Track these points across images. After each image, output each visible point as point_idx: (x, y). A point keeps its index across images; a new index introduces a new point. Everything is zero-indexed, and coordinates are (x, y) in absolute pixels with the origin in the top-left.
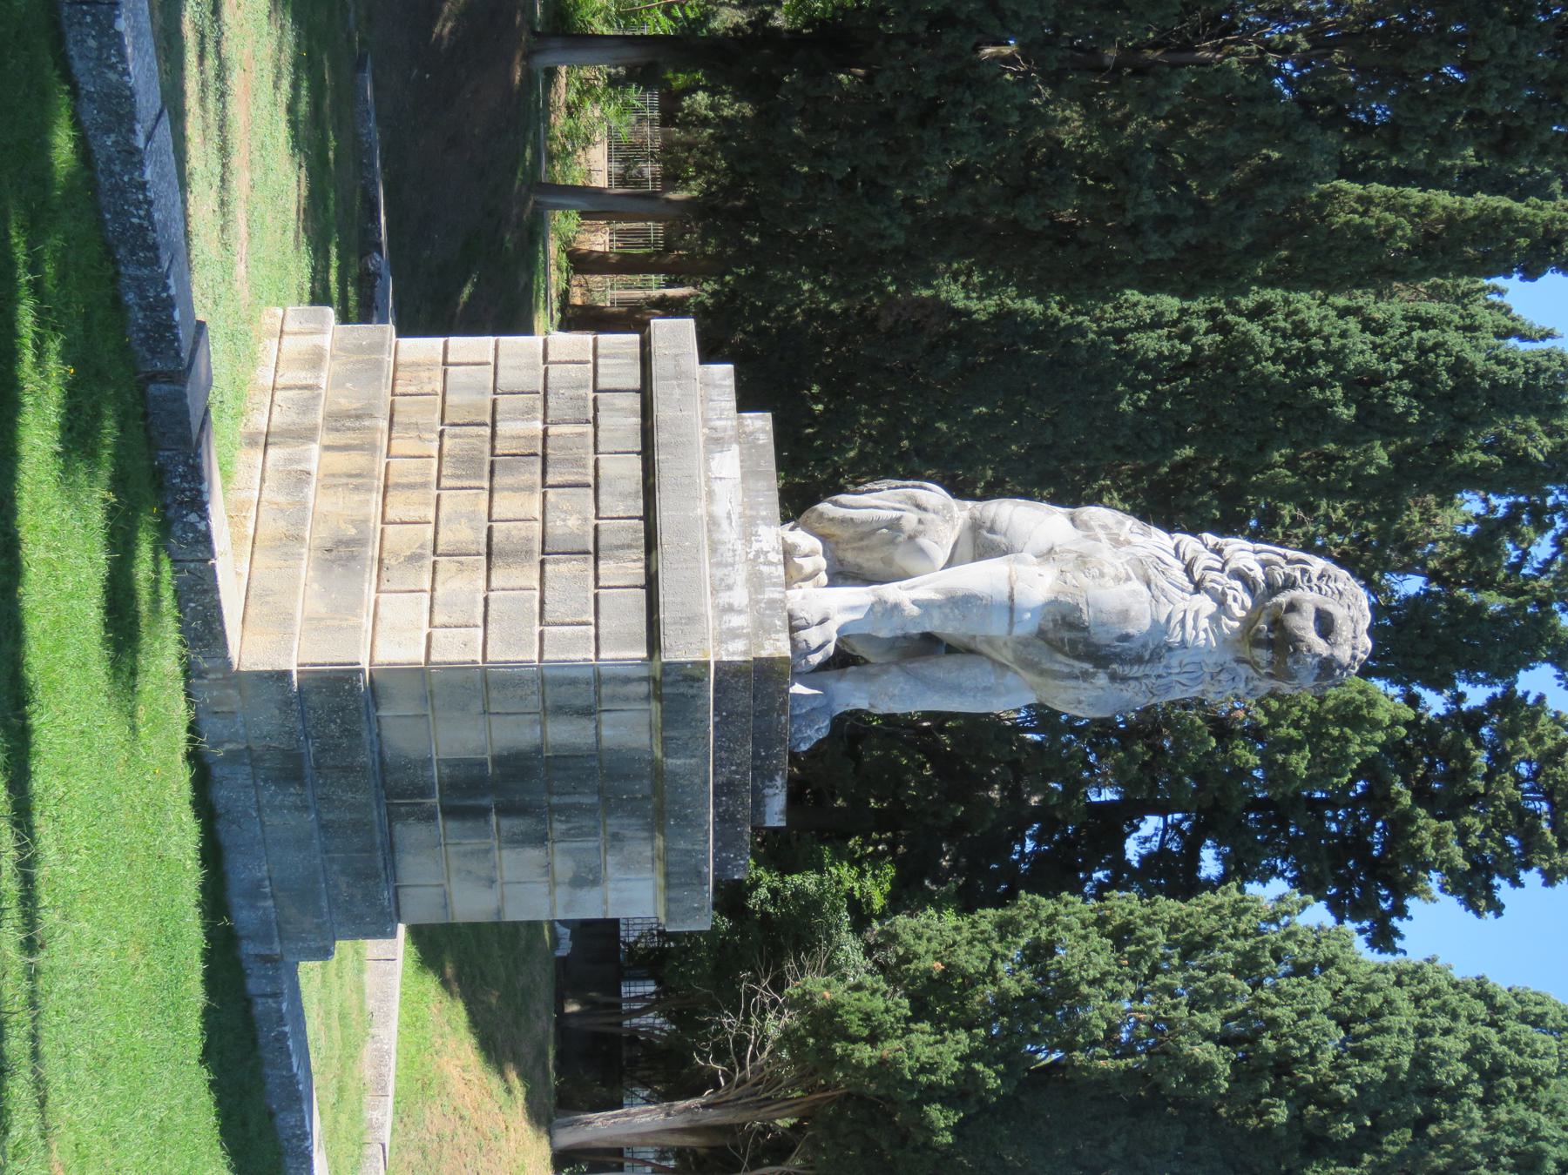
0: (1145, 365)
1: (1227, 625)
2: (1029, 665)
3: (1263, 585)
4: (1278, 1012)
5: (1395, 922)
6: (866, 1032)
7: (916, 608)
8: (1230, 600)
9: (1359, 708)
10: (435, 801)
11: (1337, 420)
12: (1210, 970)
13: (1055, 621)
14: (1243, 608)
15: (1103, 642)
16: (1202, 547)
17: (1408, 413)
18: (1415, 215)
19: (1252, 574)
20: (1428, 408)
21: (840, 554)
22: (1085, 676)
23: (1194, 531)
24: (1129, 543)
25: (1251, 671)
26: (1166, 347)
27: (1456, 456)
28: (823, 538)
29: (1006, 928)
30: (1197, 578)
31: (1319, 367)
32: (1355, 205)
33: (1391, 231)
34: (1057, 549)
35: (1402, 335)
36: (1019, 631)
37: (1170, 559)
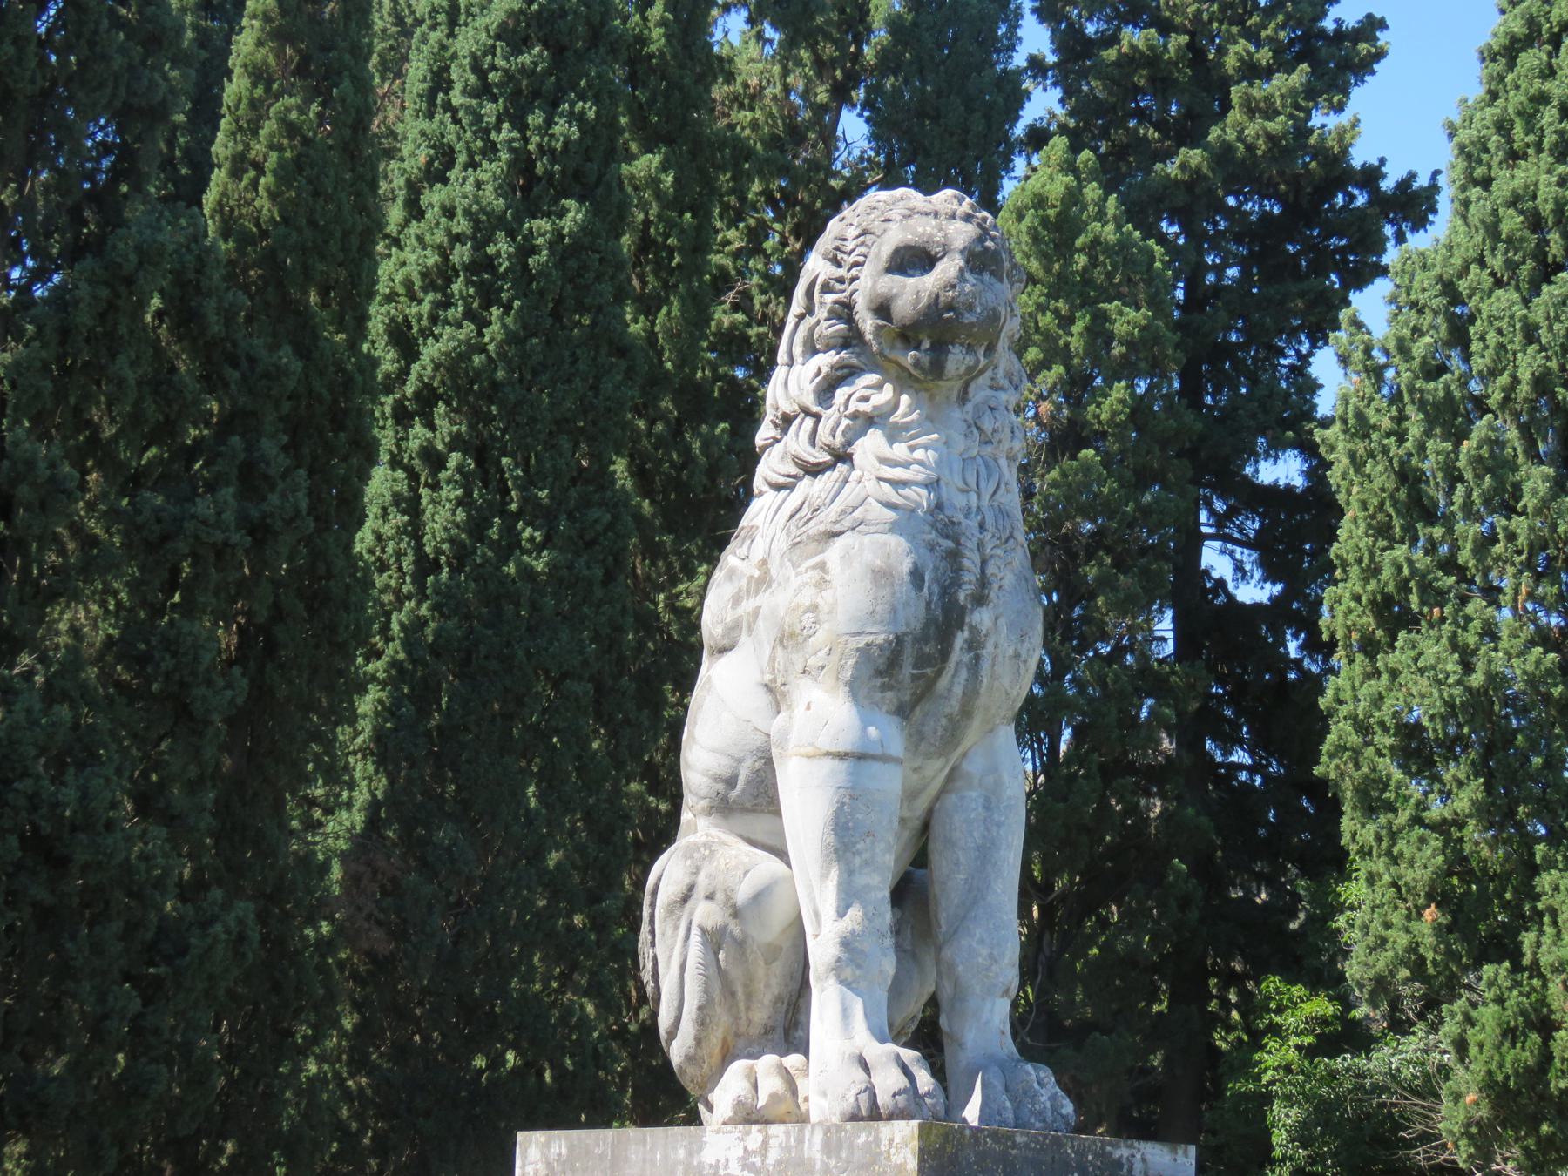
0: (477, 527)
1: (905, 415)
2: (953, 734)
3: (844, 354)
4: (1525, 374)
5: (1387, 185)
6: (1535, 1037)
7: (851, 912)
8: (864, 407)
9: (1045, 221)
11: (585, 229)
12: (1453, 478)
13: (884, 688)
14: (879, 387)
15: (922, 613)
16: (778, 447)
17: (580, 118)
18: (268, 89)
19: (825, 370)
20: (574, 86)
21: (755, 1031)
22: (974, 645)
23: (750, 459)
24: (764, 562)
25: (981, 380)
26: (451, 493)
27: (653, 48)
28: (727, 1058)
29: (1373, 801)
30: (827, 458)
31: (499, 252)
32: (245, 181)
33: (291, 129)
34: (768, 677)
35: (456, 121)
36: (897, 746)
37: (795, 498)
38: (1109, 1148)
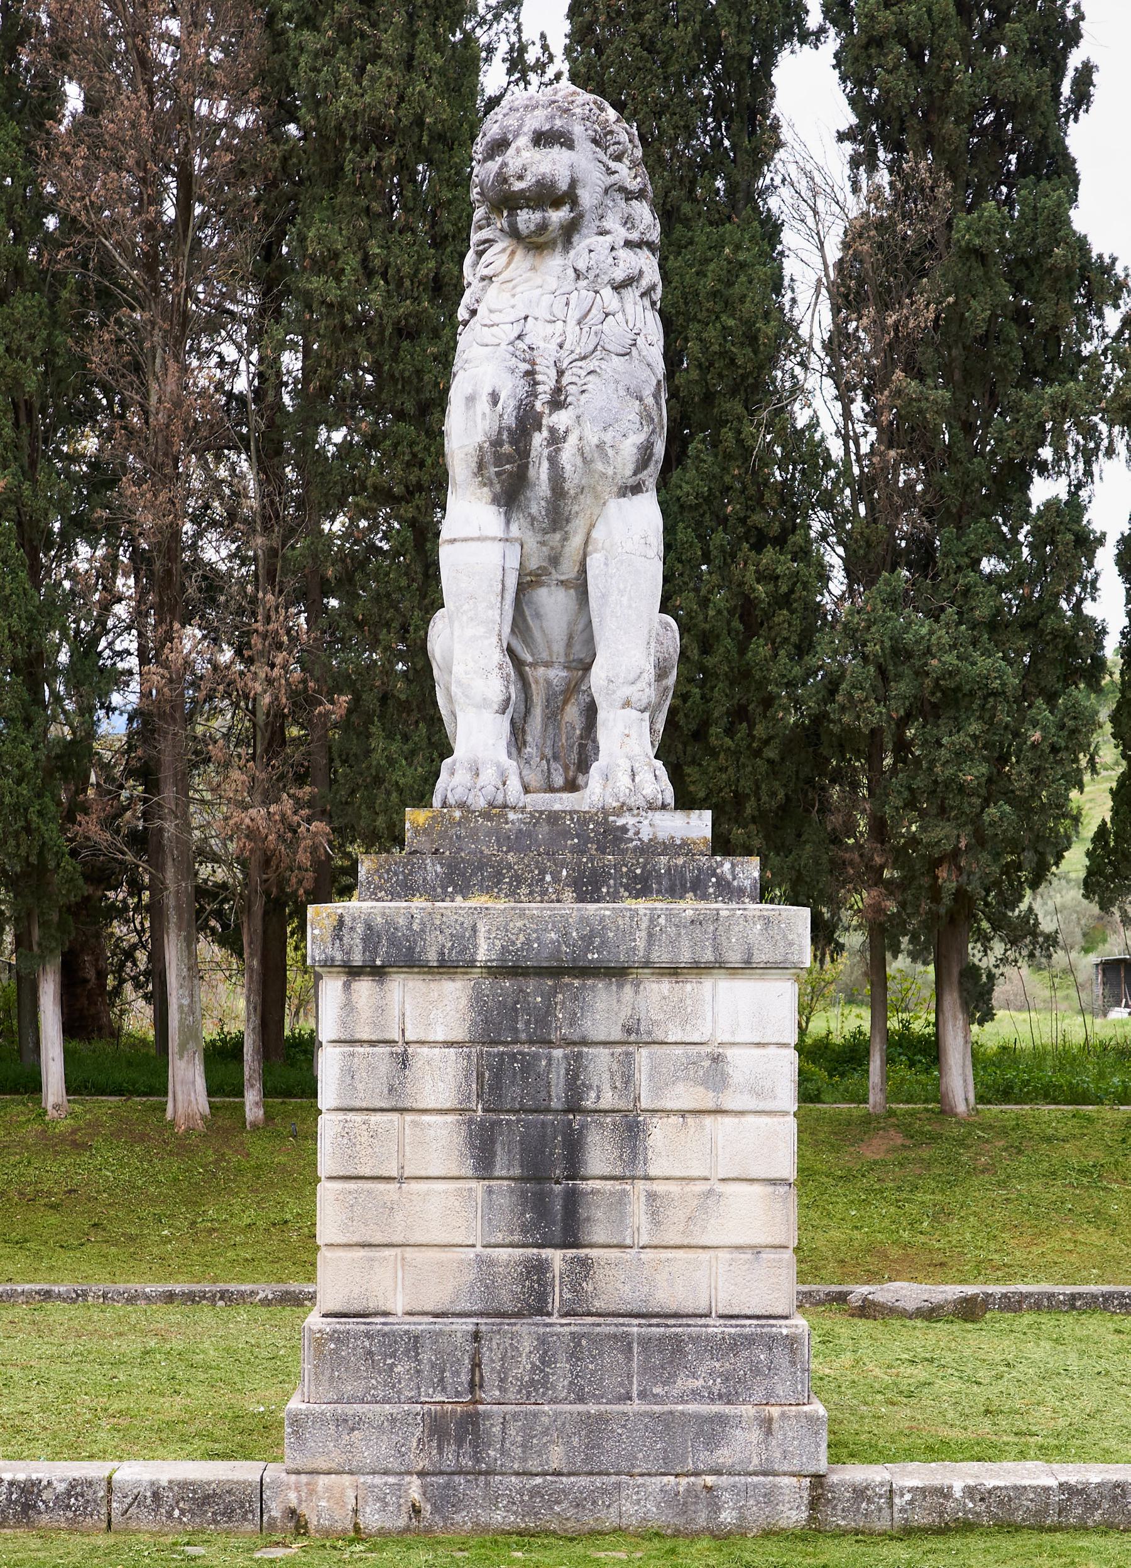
10: (556, 1257)
22: (556, 439)
38: (611, 818)
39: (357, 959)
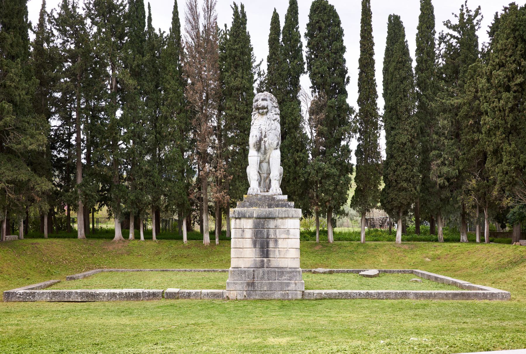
10: (265, 259)
22: (265, 142)
39: (237, 217)
